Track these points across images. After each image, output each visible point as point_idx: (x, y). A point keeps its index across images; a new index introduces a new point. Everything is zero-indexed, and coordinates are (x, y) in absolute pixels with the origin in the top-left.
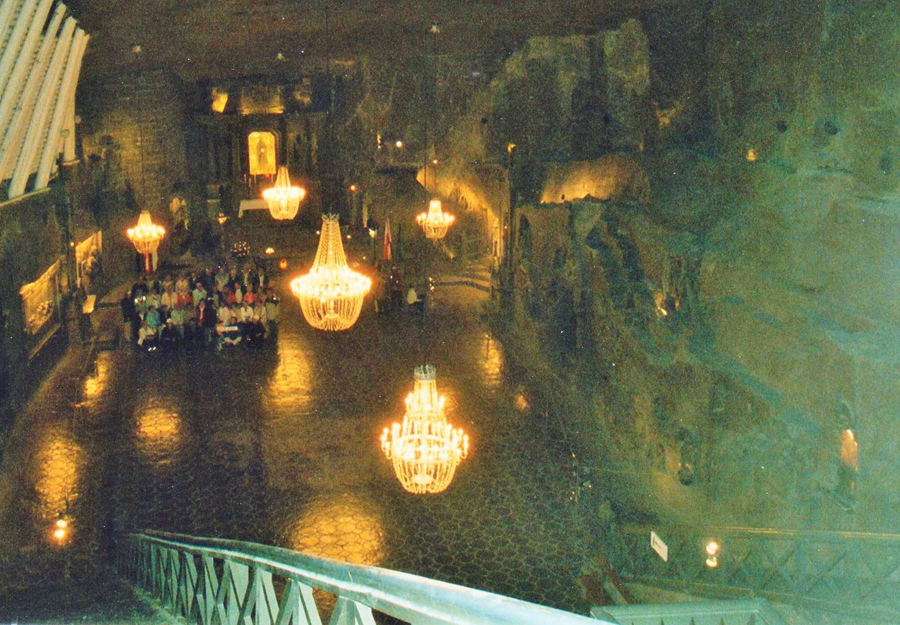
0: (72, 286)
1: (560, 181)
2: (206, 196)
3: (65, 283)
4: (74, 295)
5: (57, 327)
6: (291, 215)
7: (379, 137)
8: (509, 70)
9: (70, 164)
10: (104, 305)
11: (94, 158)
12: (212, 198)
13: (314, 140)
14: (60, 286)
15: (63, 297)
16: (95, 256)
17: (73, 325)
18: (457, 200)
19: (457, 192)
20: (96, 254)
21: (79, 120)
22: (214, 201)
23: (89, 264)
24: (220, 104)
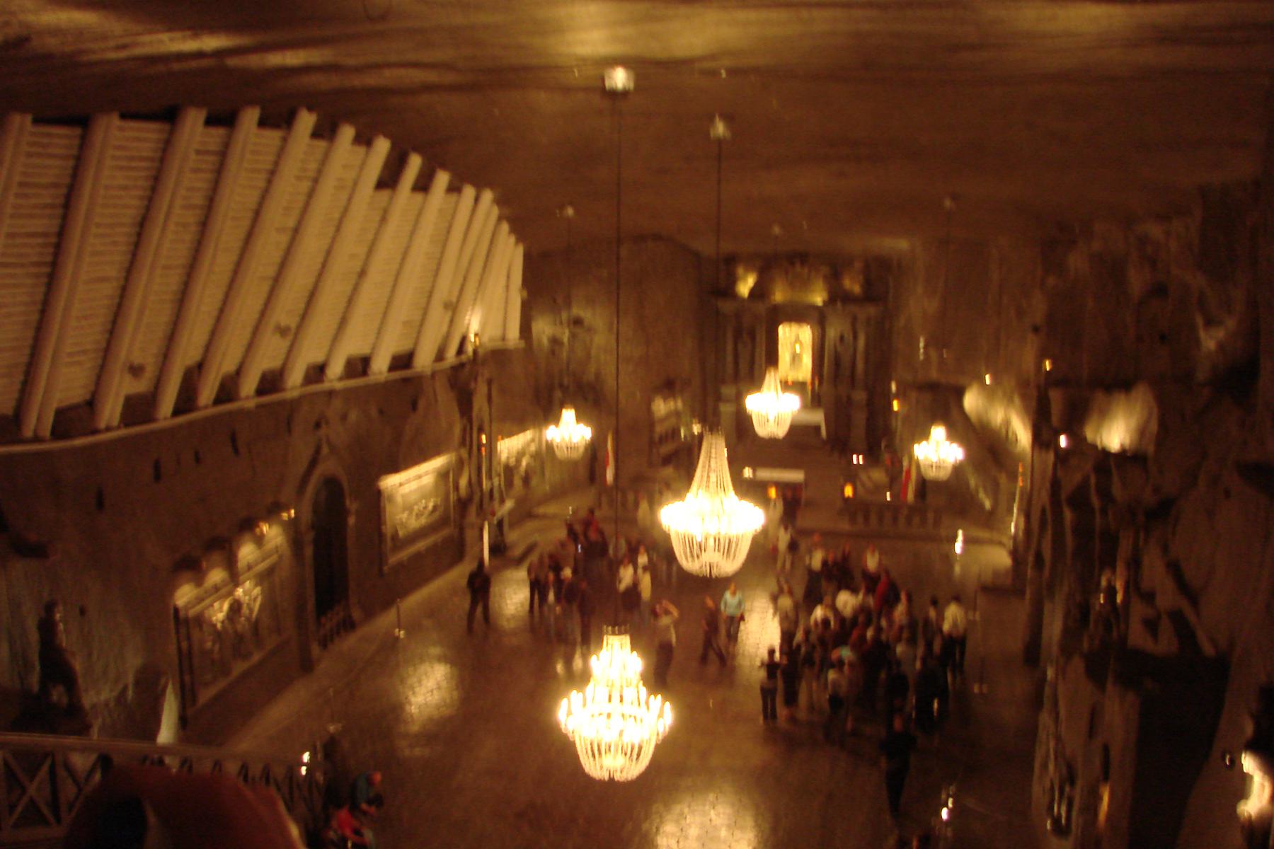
0: (475, 484)
1: (1104, 414)
3: (463, 482)
4: (477, 498)
5: (445, 532)
6: (781, 432)
11: (555, 341)
13: (861, 343)
15: (459, 500)
18: (1007, 432)
19: (1007, 423)
20: (537, 456)
21: (525, 294)
24: (745, 286)
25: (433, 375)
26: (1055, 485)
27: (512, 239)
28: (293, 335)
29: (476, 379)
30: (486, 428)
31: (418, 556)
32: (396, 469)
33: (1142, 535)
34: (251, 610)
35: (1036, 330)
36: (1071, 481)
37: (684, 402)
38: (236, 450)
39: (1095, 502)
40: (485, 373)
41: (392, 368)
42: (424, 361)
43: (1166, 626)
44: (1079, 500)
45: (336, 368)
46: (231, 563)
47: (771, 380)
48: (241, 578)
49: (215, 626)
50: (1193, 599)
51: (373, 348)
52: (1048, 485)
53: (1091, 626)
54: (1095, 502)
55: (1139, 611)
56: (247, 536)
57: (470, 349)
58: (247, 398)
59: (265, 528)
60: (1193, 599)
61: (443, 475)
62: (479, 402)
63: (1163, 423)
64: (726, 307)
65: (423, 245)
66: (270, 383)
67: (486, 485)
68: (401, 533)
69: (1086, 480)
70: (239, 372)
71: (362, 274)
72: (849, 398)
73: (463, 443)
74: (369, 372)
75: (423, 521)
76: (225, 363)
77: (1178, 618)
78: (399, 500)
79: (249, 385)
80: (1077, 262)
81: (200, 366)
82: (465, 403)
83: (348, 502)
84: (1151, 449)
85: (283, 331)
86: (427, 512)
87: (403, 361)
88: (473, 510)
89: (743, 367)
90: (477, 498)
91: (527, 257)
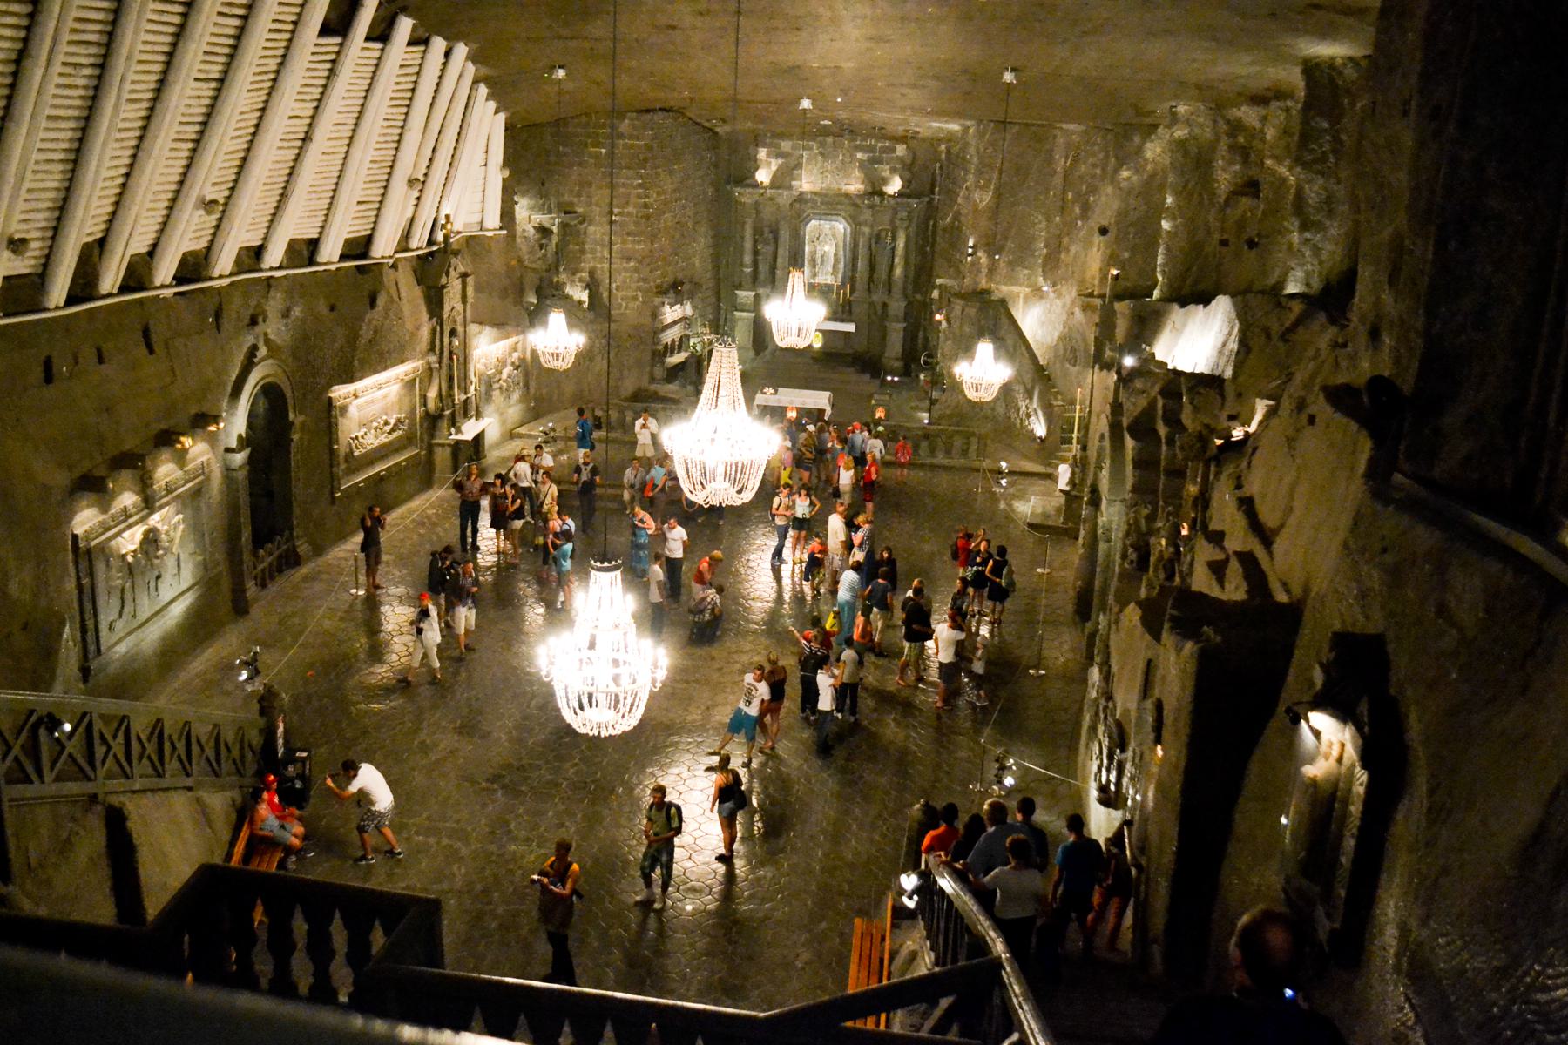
0: (445, 398)
1: (1178, 331)
2: (736, 307)
3: (432, 394)
4: (447, 412)
7: (971, 243)
8: (1149, 155)
9: (490, 234)
10: (520, 436)
11: (543, 231)
12: (742, 311)
13: (901, 243)
14: (424, 398)
15: (427, 413)
16: (517, 368)
17: (442, 457)
21: (507, 173)
22: (744, 314)
23: (504, 375)
25: (394, 266)
26: (1117, 408)
27: (492, 105)
28: (221, 210)
29: (448, 274)
30: (460, 329)
31: (378, 480)
32: (350, 378)
33: (1213, 468)
34: (171, 541)
35: (1104, 231)
36: (1134, 406)
37: (694, 307)
38: (151, 351)
39: (1162, 430)
40: (459, 265)
41: (343, 257)
42: (383, 248)
43: (1235, 569)
44: (1142, 428)
45: (275, 255)
46: (144, 486)
47: (797, 281)
48: (158, 504)
49: (123, 557)
50: (1266, 537)
51: (320, 233)
52: (1108, 409)
53: (1151, 569)
54: (1162, 430)
55: (1204, 553)
56: (165, 454)
57: (440, 236)
58: (163, 286)
59: (187, 441)
60: (1266, 537)
61: (410, 384)
62: (452, 300)
63: (1243, 342)
64: (745, 196)
65: (381, 106)
66: (193, 268)
67: (459, 397)
68: (356, 453)
69: (1152, 405)
70: (151, 253)
71: (307, 139)
72: (885, 305)
73: (432, 349)
74: (319, 260)
75: (384, 439)
76: (133, 240)
77: (1247, 559)
78: (353, 411)
79: (165, 270)
80: (1154, 150)
81: (102, 243)
82: (434, 302)
83: (291, 416)
84: (1228, 374)
85: (209, 205)
86: (388, 428)
87: (359, 248)
88: (444, 424)
89: (764, 268)
90: (447, 412)
91: (512, 131)
